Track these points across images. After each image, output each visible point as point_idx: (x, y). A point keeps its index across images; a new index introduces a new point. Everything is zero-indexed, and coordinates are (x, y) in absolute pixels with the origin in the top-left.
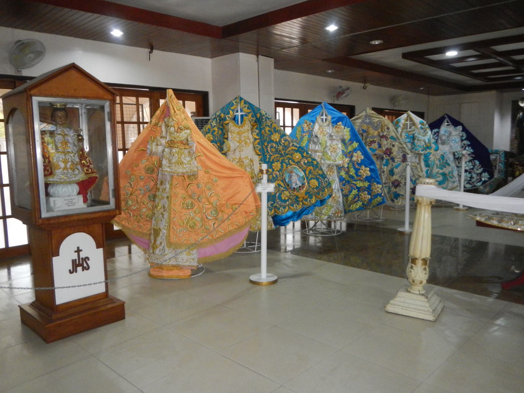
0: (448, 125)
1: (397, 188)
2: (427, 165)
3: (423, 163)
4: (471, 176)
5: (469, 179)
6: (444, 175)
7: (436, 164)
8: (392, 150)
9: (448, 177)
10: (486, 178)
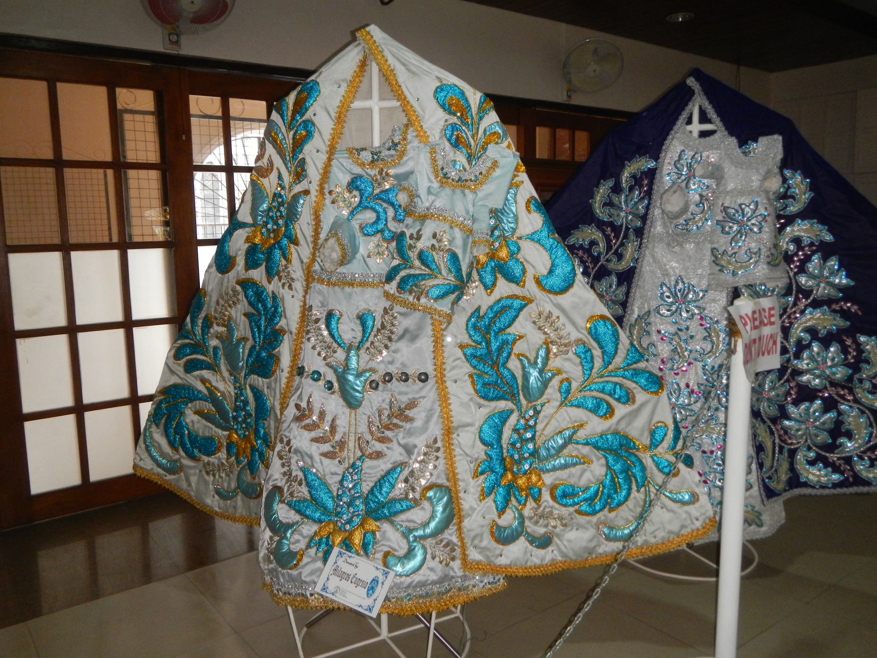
0: (704, 134)
4: (838, 423)
5: (823, 438)
7: (555, 382)
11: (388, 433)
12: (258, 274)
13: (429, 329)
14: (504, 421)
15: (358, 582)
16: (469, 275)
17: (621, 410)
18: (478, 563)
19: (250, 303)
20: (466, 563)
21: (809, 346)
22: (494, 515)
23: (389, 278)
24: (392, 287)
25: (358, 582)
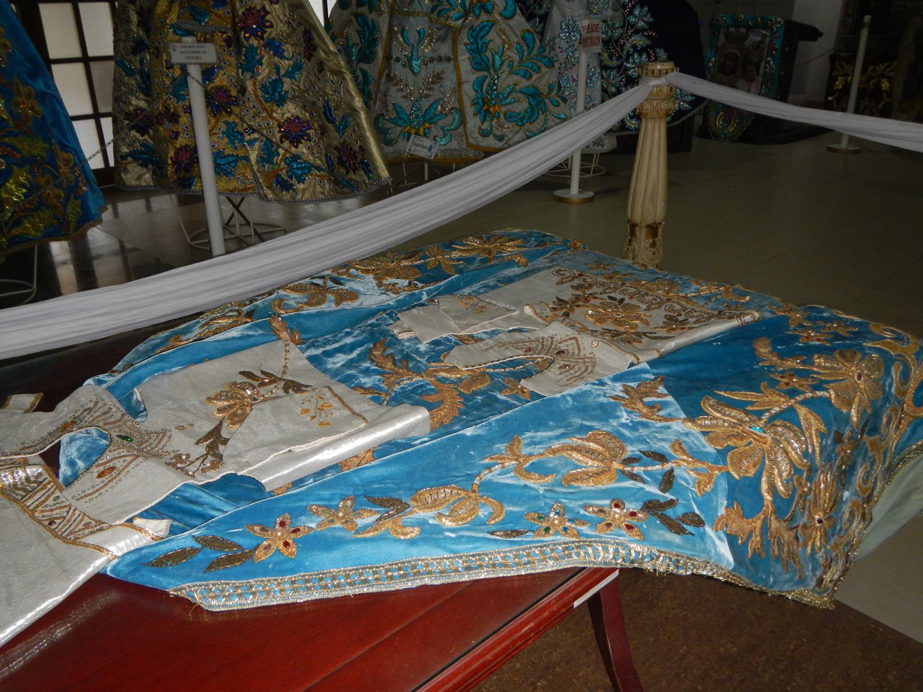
1: (300, 145)
2: (480, 65)
3: (464, 59)
6: (535, 95)
7: (507, 62)
8: (267, 13)
9: (547, 101)
10: (684, 101)
11: (432, 86)
12: (364, 10)
13: (450, 36)
14: (484, 81)
15: (424, 147)
16: (469, 9)
17: (535, 76)
18: (473, 145)
19: (359, 24)
20: (468, 144)
21: (632, 55)
22: (480, 124)
23: (432, 12)
24: (434, 16)
25: (424, 147)
